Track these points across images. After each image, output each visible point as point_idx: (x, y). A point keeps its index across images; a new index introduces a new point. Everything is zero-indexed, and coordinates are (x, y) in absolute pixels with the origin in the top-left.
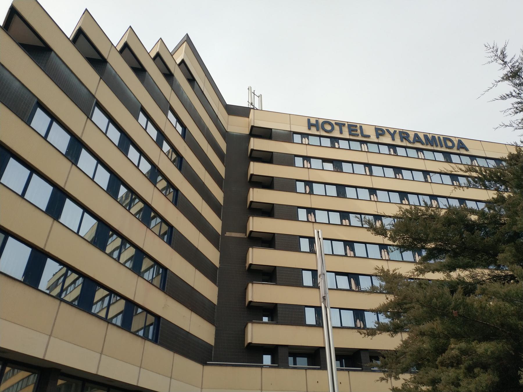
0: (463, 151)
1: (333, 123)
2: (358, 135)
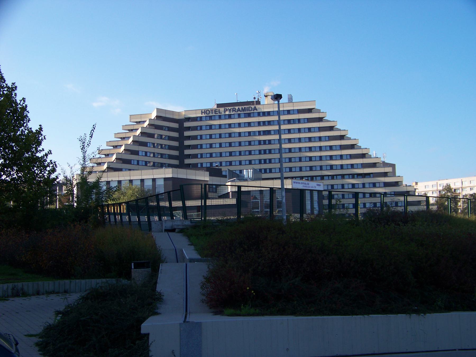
0: (255, 111)
1: (210, 110)
2: (217, 113)
